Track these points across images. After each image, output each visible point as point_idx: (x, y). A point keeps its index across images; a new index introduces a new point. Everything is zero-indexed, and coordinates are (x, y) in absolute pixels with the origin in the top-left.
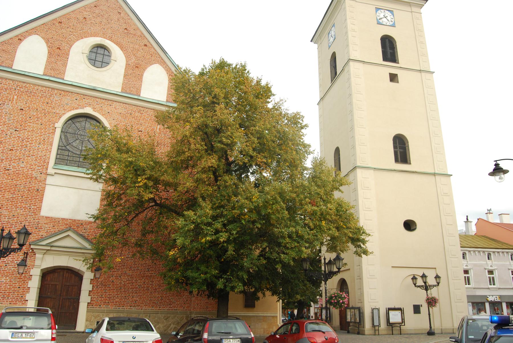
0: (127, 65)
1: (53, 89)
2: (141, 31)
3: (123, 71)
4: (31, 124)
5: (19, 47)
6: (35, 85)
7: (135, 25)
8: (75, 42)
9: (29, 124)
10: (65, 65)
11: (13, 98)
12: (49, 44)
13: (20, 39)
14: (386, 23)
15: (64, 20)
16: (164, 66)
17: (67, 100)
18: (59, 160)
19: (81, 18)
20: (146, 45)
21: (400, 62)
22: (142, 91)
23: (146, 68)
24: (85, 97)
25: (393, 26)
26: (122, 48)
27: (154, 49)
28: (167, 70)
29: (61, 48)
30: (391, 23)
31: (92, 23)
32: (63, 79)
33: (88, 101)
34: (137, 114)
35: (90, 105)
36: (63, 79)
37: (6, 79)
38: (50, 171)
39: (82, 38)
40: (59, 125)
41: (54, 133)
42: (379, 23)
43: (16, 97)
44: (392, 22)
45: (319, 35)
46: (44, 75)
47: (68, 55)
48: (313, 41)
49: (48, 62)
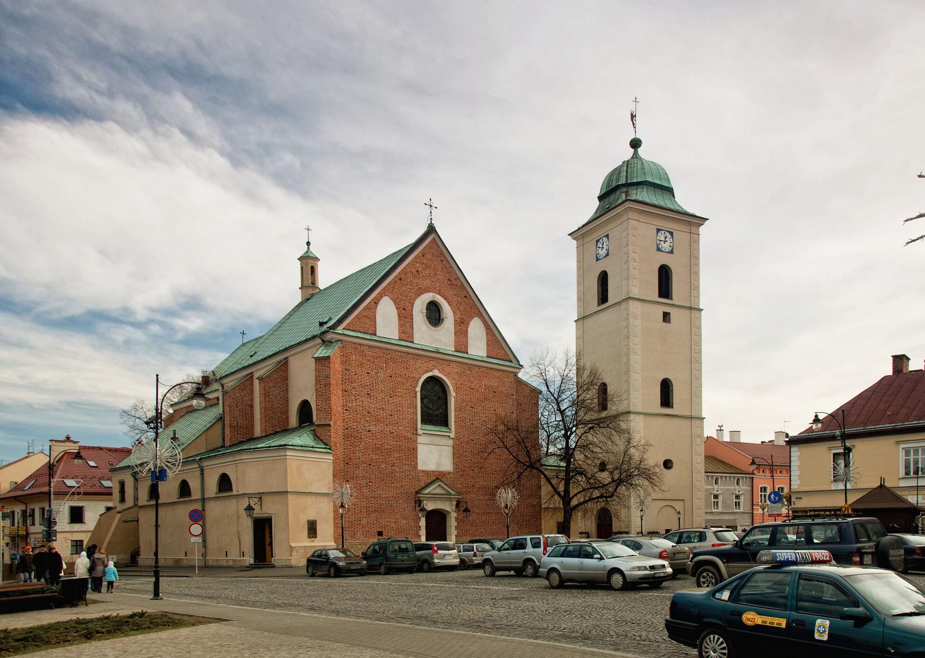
0: (455, 320)
1: (408, 354)
2: (460, 281)
3: (453, 328)
4: (399, 390)
5: (377, 311)
6: (395, 351)
7: (456, 274)
8: (414, 301)
9: (398, 390)
10: (412, 328)
11: (383, 366)
12: (397, 305)
13: (376, 302)
14: (665, 250)
15: (402, 277)
16: (482, 318)
17: (419, 363)
18: (424, 421)
19: (414, 270)
20: (466, 297)
21: (674, 296)
22: (469, 348)
23: (469, 323)
24: (431, 359)
25: (671, 252)
26: (448, 302)
27: (472, 300)
28: (484, 323)
29: (406, 309)
30: (670, 249)
31: (423, 276)
32: (413, 342)
33: (432, 363)
34: (468, 372)
35: (435, 367)
36: (413, 342)
37: (375, 347)
38: (420, 432)
39: (419, 296)
40: (418, 389)
41: (416, 397)
42: (659, 249)
43: (384, 364)
44: (670, 246)
45: (582, 234)
46: (400, 339)
47: (412, 315)
48: (572, 235)
49: (400, 325)
